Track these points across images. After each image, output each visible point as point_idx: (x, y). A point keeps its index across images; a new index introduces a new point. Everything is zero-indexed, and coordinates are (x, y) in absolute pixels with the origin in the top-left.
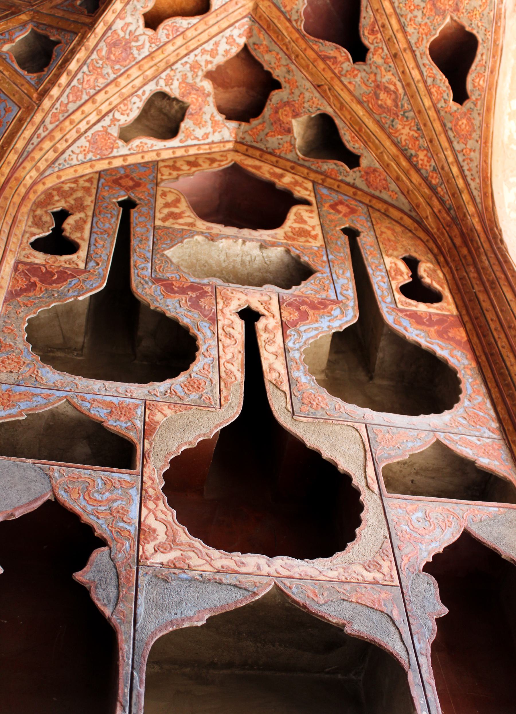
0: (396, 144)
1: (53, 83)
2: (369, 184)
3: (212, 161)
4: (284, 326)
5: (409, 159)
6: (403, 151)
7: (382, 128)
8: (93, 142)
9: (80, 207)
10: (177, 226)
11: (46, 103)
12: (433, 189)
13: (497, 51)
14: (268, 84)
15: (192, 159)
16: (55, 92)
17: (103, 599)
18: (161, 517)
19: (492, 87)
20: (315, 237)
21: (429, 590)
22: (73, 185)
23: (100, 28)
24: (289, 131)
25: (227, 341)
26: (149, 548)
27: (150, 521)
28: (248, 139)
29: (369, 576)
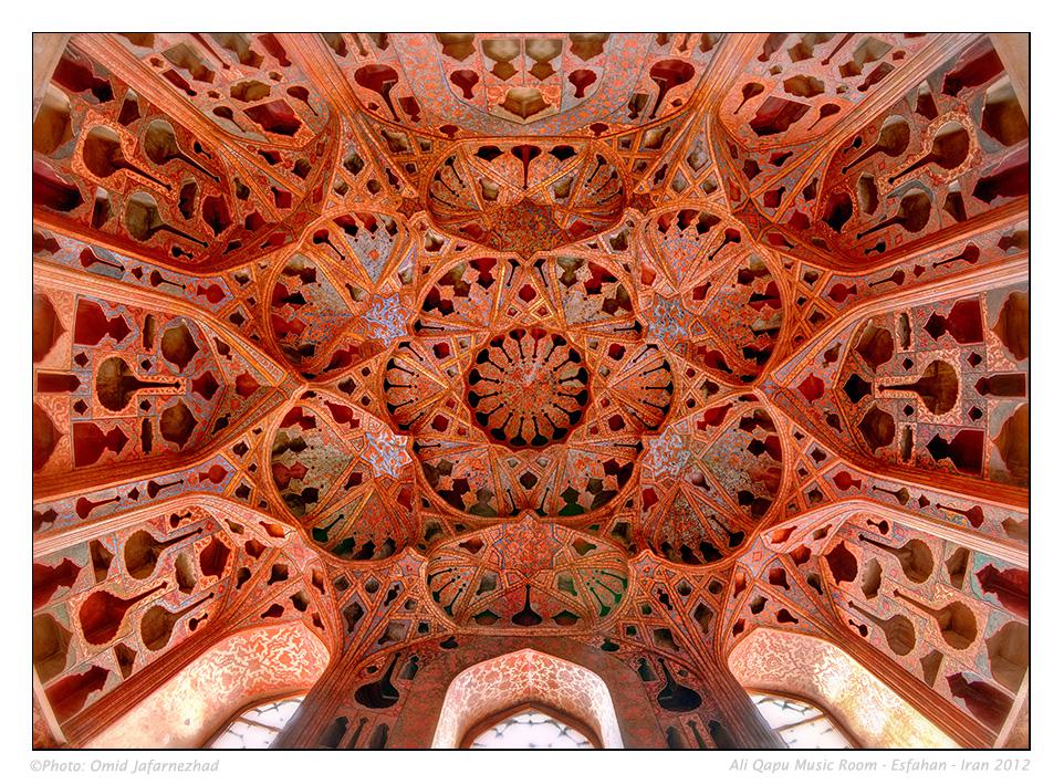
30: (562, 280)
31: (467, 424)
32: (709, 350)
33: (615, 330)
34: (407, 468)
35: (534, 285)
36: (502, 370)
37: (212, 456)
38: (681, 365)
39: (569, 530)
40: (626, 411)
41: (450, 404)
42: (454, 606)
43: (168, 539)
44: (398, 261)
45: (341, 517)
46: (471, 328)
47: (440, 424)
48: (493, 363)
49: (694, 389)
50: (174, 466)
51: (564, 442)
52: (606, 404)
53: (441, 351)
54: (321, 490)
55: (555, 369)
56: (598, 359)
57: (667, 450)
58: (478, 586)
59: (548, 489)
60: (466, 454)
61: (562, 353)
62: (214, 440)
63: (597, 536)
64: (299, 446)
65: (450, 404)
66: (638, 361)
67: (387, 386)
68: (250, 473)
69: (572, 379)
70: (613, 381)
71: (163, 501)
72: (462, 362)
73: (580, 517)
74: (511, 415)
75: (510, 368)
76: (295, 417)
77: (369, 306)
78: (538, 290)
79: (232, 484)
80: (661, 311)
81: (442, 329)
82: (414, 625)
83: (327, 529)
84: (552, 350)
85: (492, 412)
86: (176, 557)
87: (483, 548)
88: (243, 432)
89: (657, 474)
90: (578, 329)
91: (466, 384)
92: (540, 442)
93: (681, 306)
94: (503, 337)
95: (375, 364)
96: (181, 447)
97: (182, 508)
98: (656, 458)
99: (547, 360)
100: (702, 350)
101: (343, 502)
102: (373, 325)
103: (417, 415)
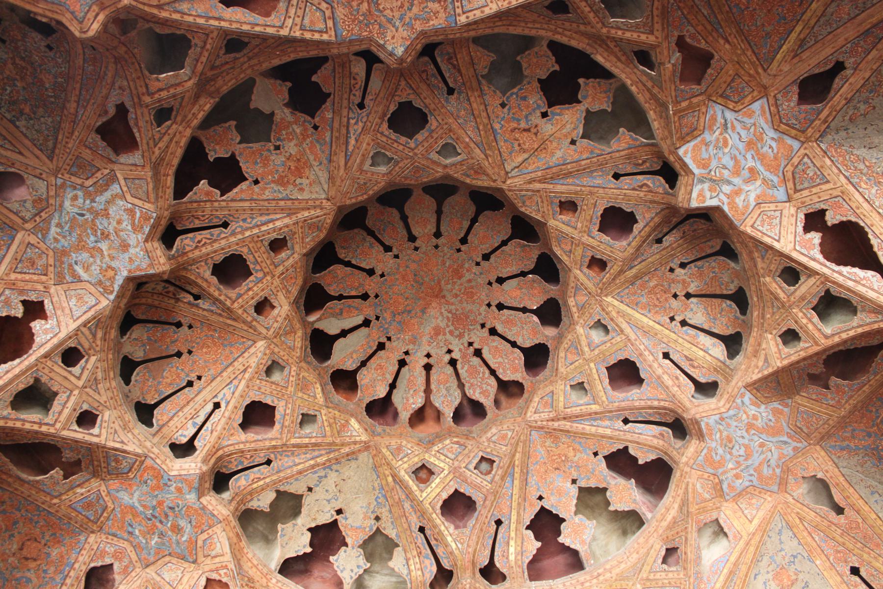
30: (390, 545)
31: (558, 223)
32: (56, 473)
33: (269, 462)
35: (446, 529)
36: (493, 332)
38: (117, 431)
39: (297, 34)
40: (216, 301)
41: (598, 264)
44: (731, 573)
46: (567, 425)
47: (616, 220)
48: (514, 344)
49: (72, 390)
51: (340, 209)
52: (263, 306)
53: (626, 373)
55: (381, 346)
56: (298, 390)
57: (104, 246)
59: (361, 106)
60: (554, 161)
61: (373, 384)
63: (224, 32)
65: (598, 264)
66: (210, 407)
67: (740, 299)
69: (344, 333)
70: (257, 354)
72: (580, 353)
73: (276, 62)
74: (464, 241)
75: (479, 337)
77: (787, 471)
78: (438, 519)
80: (176, 529)
81: (626, 421)
84: (393, 386)
85: (504, 243)
89: (115, 189)
90: (346, 450)
91: (566, 303)
92: (395, 197)
93: (137, 547)
94: (497, 403)
95: (770, 353)
98: (126, 225)
99: (402, 363)
100: (71, 469)
101: (850, 32)
102: (775, 431)
103: (668, 240)
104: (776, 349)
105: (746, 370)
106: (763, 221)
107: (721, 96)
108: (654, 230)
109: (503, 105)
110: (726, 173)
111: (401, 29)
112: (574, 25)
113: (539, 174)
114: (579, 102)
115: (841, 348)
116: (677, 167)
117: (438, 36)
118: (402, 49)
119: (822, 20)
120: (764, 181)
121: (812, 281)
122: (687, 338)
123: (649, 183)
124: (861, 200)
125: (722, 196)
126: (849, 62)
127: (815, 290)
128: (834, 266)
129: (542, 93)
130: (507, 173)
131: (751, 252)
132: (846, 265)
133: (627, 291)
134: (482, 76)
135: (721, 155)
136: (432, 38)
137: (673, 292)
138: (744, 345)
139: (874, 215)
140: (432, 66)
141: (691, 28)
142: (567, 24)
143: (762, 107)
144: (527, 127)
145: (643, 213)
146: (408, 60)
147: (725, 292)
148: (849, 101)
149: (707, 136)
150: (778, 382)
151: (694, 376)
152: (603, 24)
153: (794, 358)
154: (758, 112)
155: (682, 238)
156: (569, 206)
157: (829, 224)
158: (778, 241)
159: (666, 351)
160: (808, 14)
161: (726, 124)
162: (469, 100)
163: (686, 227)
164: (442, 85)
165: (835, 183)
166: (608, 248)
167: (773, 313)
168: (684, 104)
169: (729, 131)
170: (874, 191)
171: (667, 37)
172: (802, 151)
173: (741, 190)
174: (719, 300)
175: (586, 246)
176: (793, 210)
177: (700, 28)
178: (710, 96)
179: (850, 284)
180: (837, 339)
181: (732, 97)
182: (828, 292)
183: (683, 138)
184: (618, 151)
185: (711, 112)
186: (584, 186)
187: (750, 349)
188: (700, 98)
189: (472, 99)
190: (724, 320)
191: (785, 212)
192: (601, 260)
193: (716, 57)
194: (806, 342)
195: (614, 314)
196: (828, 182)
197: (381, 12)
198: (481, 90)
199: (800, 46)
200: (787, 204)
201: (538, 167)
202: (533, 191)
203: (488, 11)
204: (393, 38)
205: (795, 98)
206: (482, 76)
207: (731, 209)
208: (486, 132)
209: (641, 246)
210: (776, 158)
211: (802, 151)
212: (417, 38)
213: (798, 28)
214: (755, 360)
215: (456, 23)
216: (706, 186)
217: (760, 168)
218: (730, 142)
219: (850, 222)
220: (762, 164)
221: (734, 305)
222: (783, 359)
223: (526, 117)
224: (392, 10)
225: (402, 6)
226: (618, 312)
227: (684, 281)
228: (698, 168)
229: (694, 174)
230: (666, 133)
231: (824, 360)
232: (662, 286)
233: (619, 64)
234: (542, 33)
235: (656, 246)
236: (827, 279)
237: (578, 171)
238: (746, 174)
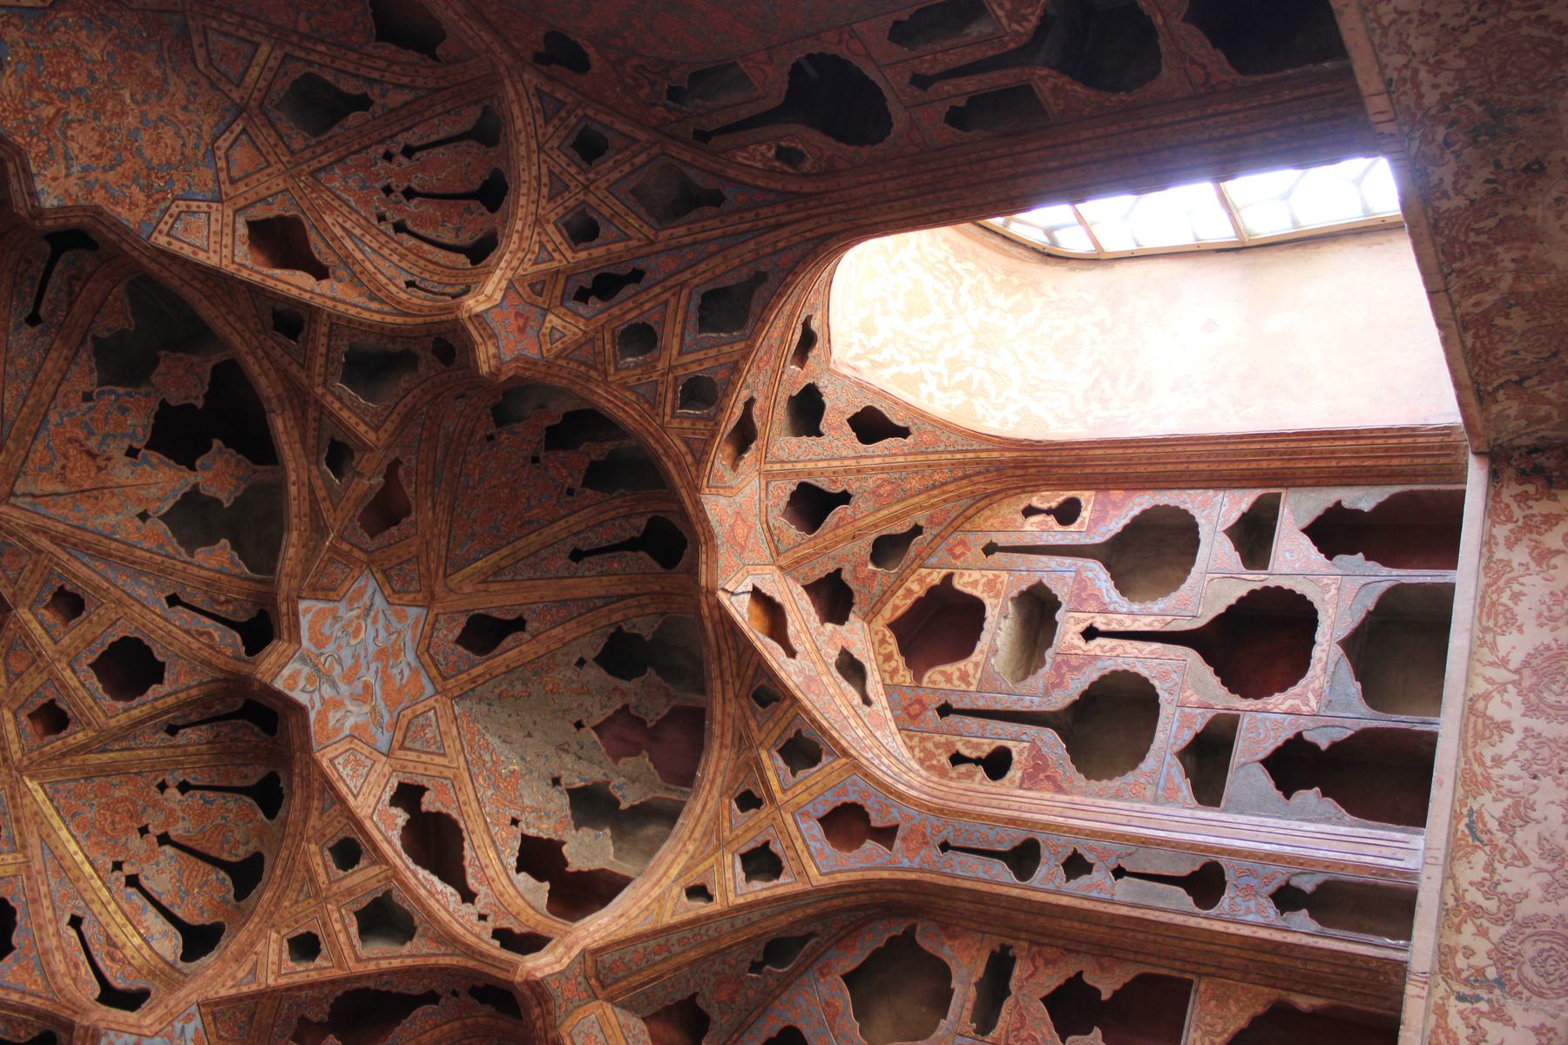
0: (920, 493)
1: (837, 743)
2: (940, 524)
3: (883, 642)
4: (1104, 611)
5: (934, 487)
6: (927, 489)
7: (904, 499)
8: (877, 727)
9: (948, 744)
10: (978, 676)
11: (852, 752)
12: (965, 477)
13: (883, 394)
14: (834, 578)
15: (881, 658)
16: (844, 744)
17: (1340, 735)
18: (1280, 701)
19: (907, 407)
20: (997, 577)
21: (1343, 560)
22: (917, 750)
23: (799, 694)
24: (875, 573)
25: (1119, 650)
26: (1305, 709)
27: (1284, 707)
28: (866, 609)
29: (1333, 591)
34: (324, 590)
37: (842, 878)
42: (458, 129)
43: (1032, 730)
45: (577, 555)
47: (129, 666)
50: (951, 893)
54: (590, 654)
58: (355, 119)
62: (821, 916)
64: (591, 805)
65: (53, 718)
68: (760, 792)
71: (1012, 821)
76: (580, 893)
79: (819, 787)
82: (608, 170)
83: (631, 545)
86: (1030, 680)
87: (259, 213)
88: (740, 908)
96: (913, 927)
97: (967, 784)
103: (188, 735)
104: (276, 959)
105: (213, 978)
106: (347, 762)
107: (384, 572)
108: (178, 707)
109: (87, 397)
110: (337, 670)
111: (73, 180)
112: (287, 359)
113: (61, 528)
114: (192, 468)
115: (371, 984)
116: (285, 622)
117: (110, 229)
118: (55, 203)
119: (532, 559)
120: (374, 708)
121: (376, 870)
122: (126, 906)
123: (216, 635)
124: (472, 796)
125: (316, 697)
126: (532, 626)
127: (374, 884)
128: (409, 862)
129: (152, 421)
130: (12, 494)
131: (310, 797)
132: (424, 867)
133: (72, 785)
134: (94, 338)
135: (344, 643)
136: (100, 227)
137: (145, 821)
138: (224, 941)
139: (480, 821)
140: (43, 266)
141: (414, 461)
142: (278, 352)
143: (418, 619)
144: (95, 450)
145: (179, 674)
146: (48, 223)
147: (225, 857)
148: (510, 671)
149: (342, 607)
150: (251, 1017)
151: (108, 974)
152: (325, 381)
153: (298, 979)
154: (410, 621)
155: (208, 742)
156: (70, 604)
157: (424, 808)
158: (356, 797)
159: (79, 913)
160: (523, 542)
161: (369, 609)
162: (47, 351)
163: (225, 728)
164: (30, 301)
165: (451, 761)
166: (90, 701)
167: (296, 902)
168: (345, 547)
169: (369, 621)
170: (489, 793)
171: (388, 447)
172: (431, 702)
173: (342, 703)
174: (209, 867)
175: (54, 679)
176: (387, 769)
177: (422, 467)
178: (373, 562)
179: (423, 892)
180: (372, 967)
181: (396, 582)
182: (388, 893)
183: (315, 590)
184: (199, 566)
185: (361, 582)
186: (115, 586)
187: (233, 947)
188: (363, 556)
189: (53, 355)
190: (201, 900)
191: (378, 766)
192: (63, 714)
193: (413, 517)
194: (325, 959)
195: (27, 812)
196: (444, 755)
197: (66, 137)
198: (76, 354)
199: (495, 574)
200: (384, 759)
201: (66, 518)
202: (31, 546)
203: (202, 257)
204: (55, 179)
205: (457, 632)
206: (94, 338)
207: (318, 721)
208: (32, 413)
209: (142, 722)
210: (400, 691)
211: (431, 702)
212: (84, 209)
213: (504, 552)
214: (235, 967)
215: (149, 237)
216: (306, 670)
217: (378, 692)
218: (362, 635)
219: (448, 817)
220: (383, 689)
221: (229, 881)
222: (279, 975)
223: (106, 436)
224: (81, 148)
225: (98, 157)
226: (36, 814)
227: (172, 811)
228: (310, 640)
229: (300, 644)
230: (299, 570)
231: (337, 999)
232: (134, 803)
233: (298, 446)
234: (236, 340)
235: (164, 735)
236: (396, 874)
237: (123, 559)
238: (358, 685)
